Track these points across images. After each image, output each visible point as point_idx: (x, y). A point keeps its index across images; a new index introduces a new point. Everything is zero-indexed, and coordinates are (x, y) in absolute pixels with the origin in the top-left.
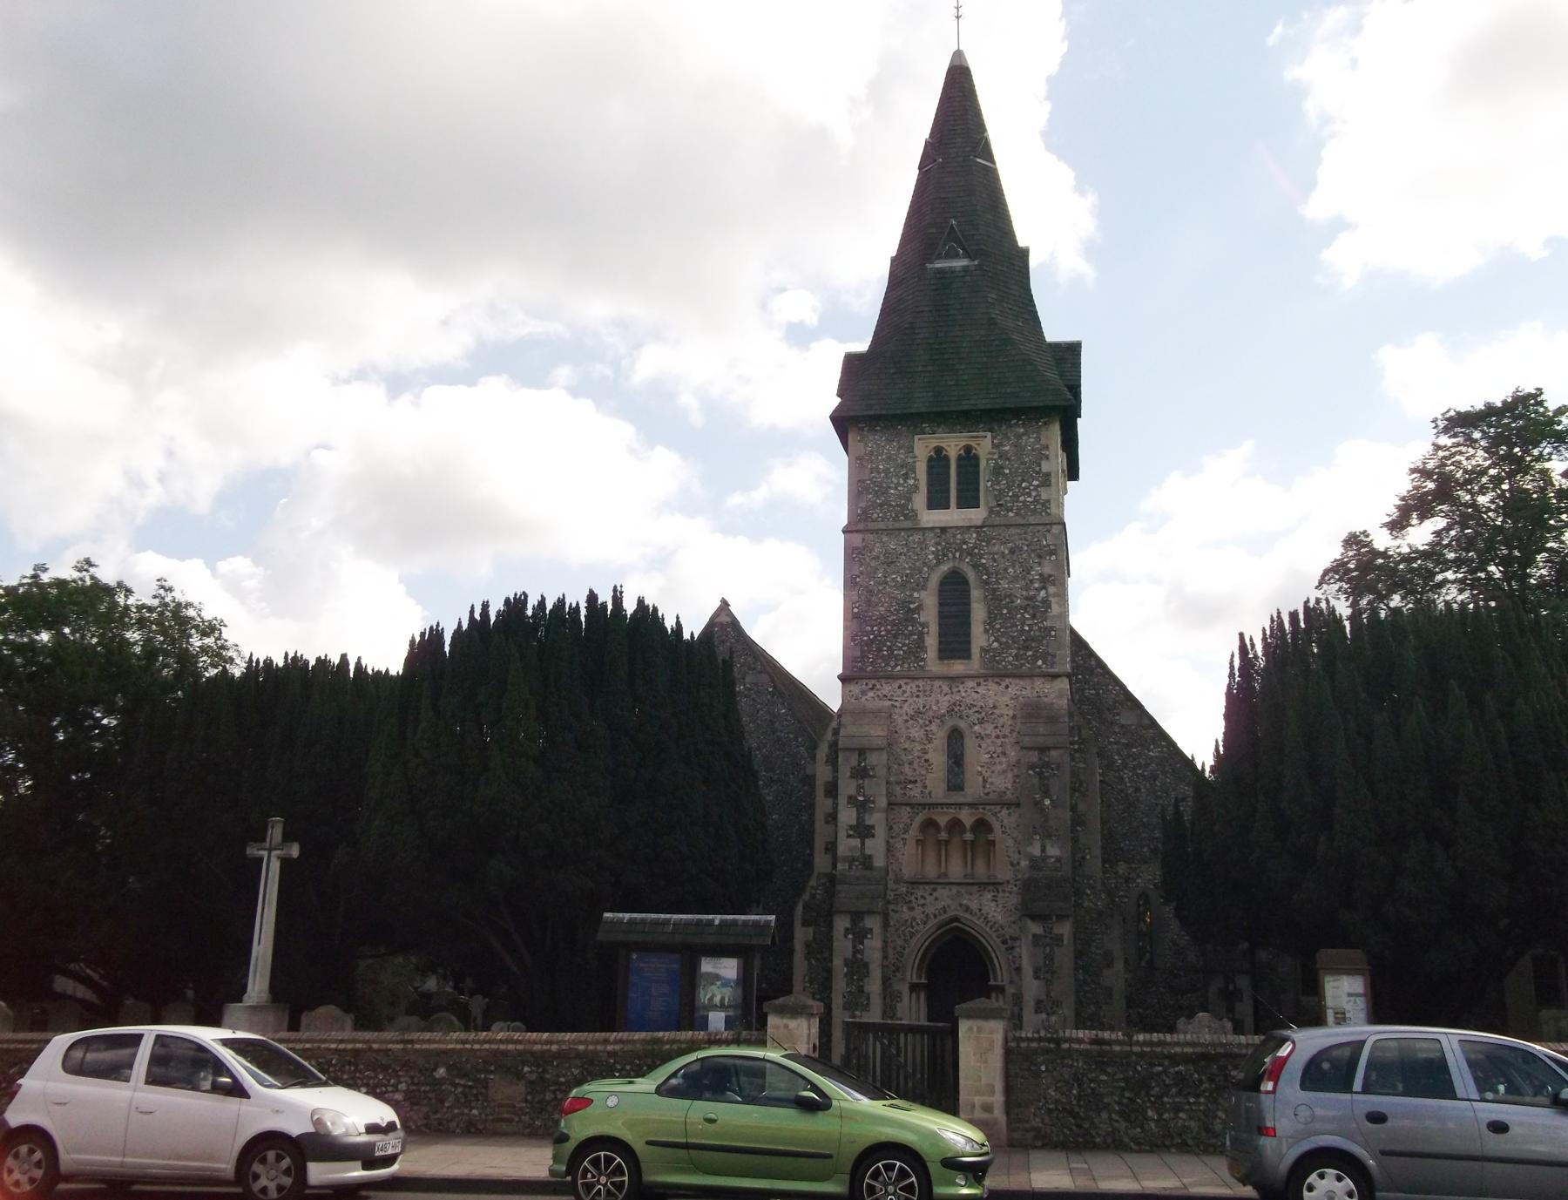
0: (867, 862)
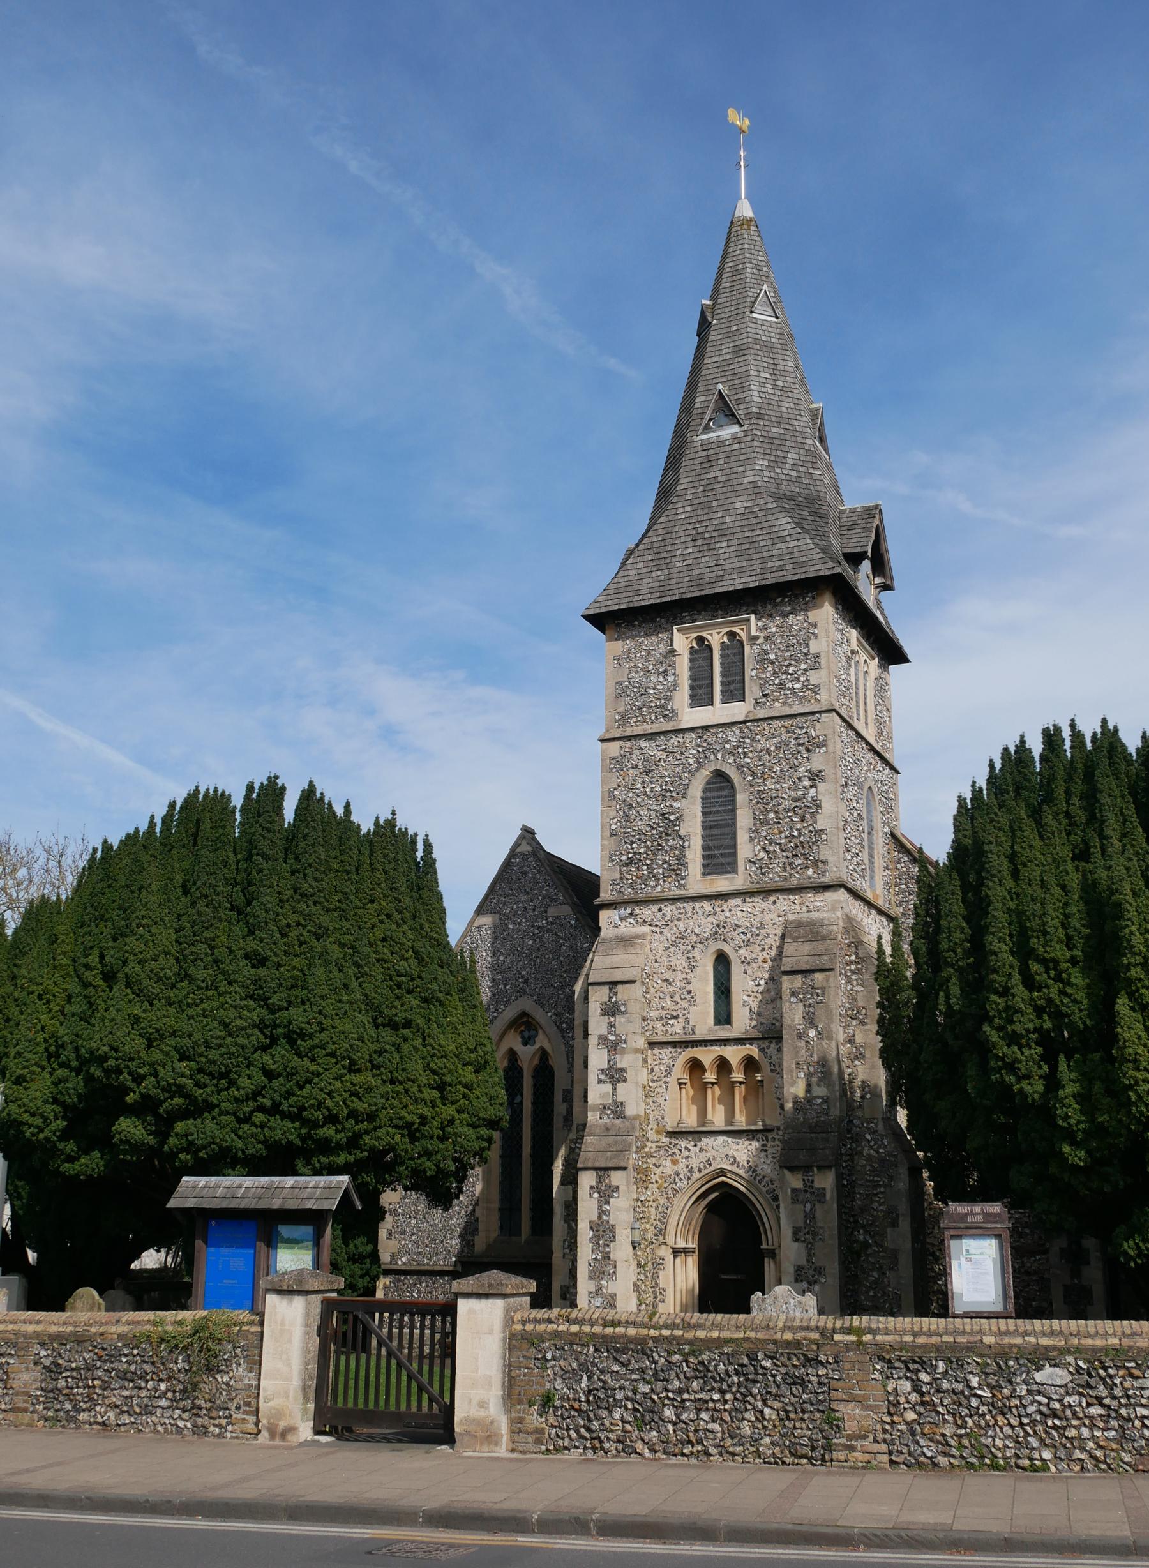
0: (618, 1110)
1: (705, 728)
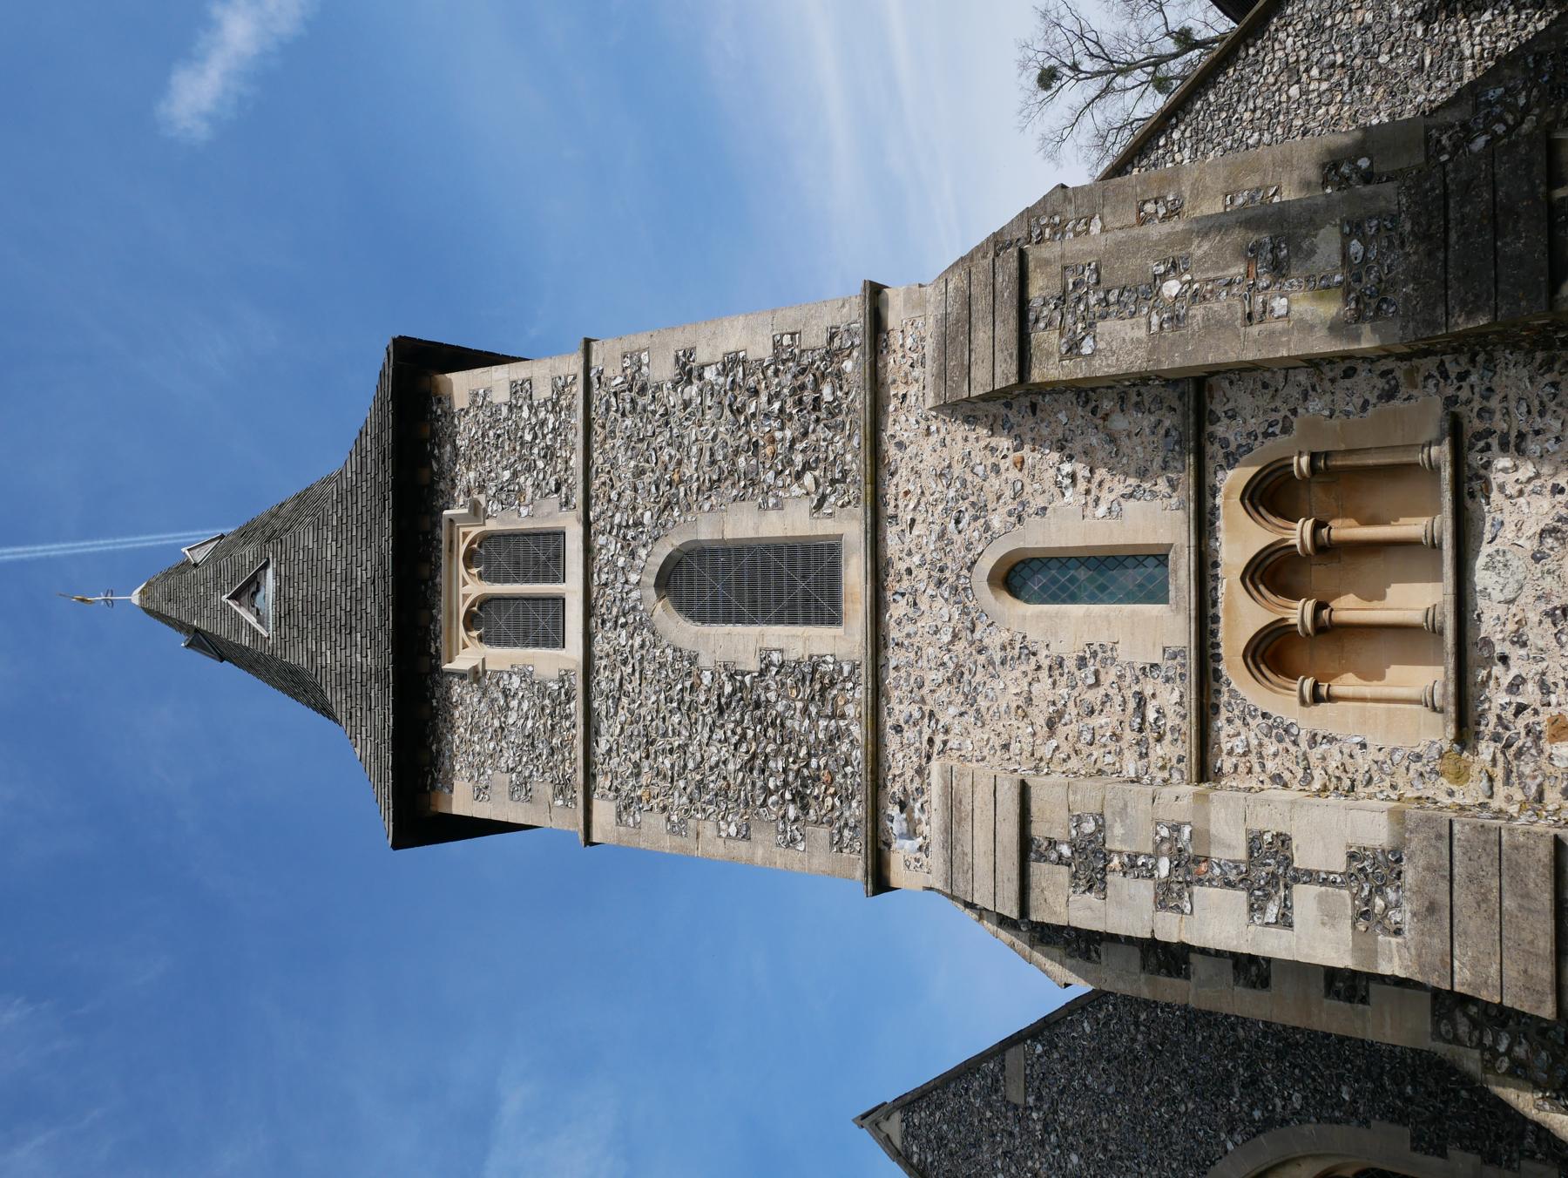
0: (1372, 872)
1: (589, 610)
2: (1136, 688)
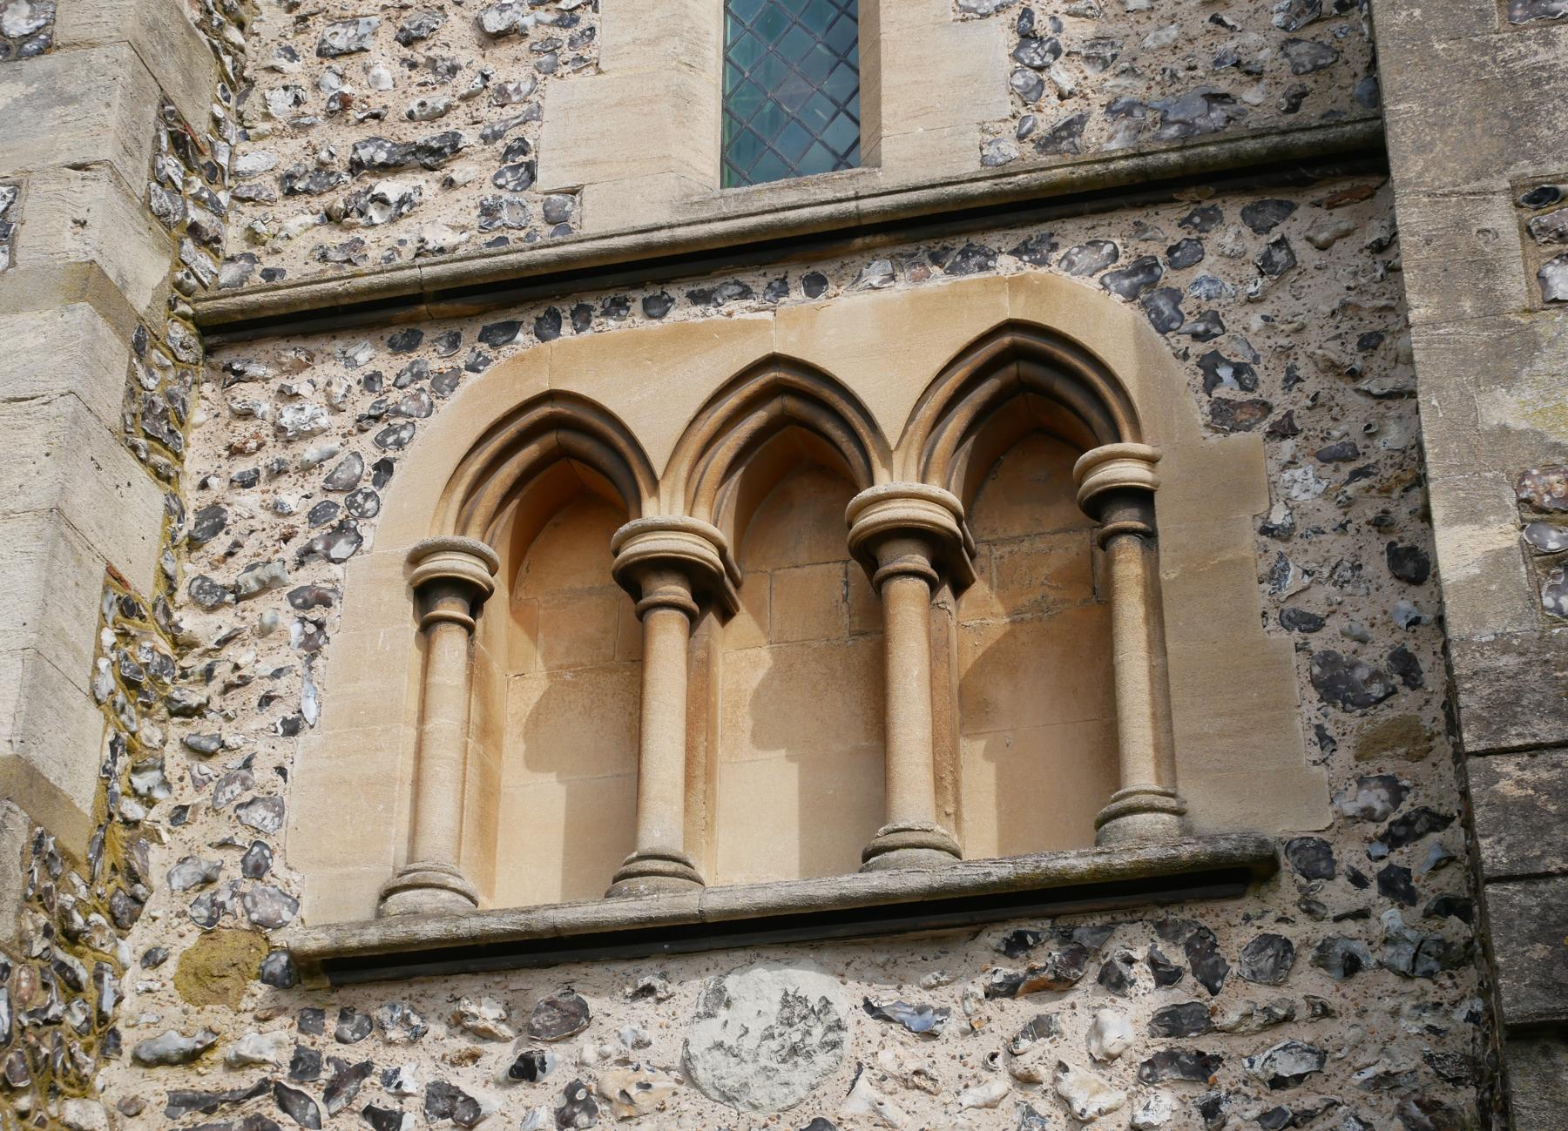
2: (469, 137)
